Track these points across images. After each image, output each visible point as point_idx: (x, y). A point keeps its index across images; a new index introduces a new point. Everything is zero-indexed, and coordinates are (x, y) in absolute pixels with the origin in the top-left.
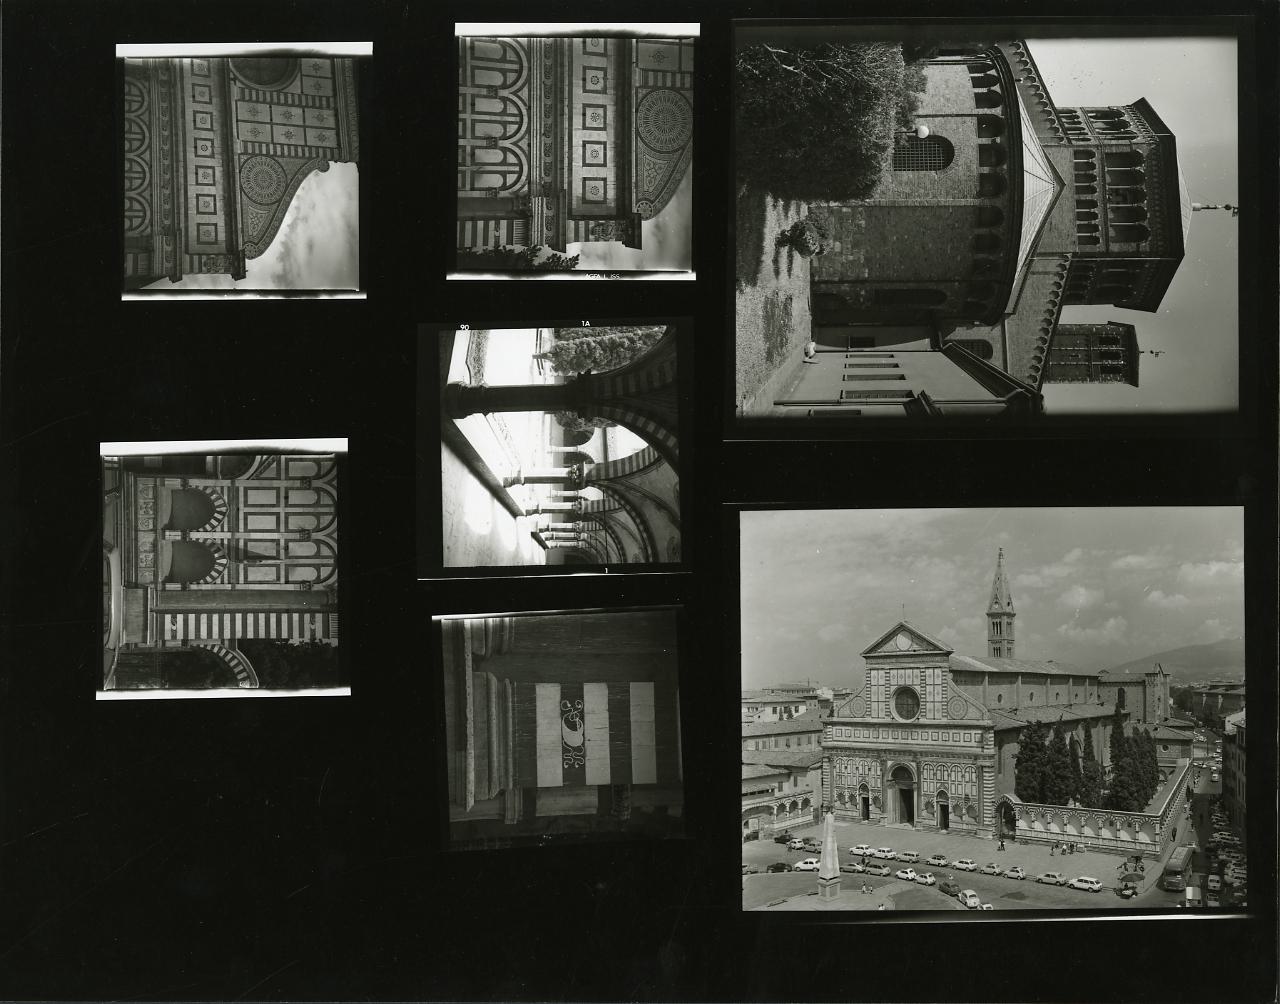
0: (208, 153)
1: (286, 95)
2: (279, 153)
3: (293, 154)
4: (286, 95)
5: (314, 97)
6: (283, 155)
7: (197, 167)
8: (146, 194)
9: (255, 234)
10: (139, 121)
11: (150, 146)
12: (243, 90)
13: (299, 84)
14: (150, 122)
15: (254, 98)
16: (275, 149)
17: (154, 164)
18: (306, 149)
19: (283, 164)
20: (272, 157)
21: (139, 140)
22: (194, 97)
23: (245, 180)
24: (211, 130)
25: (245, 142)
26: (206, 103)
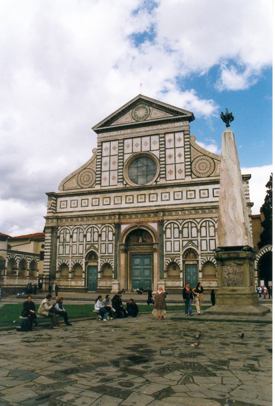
0: (193, 192)
1: (160, 158)
2: (189, 160)
3: (189, 153)
4: (160, 158)
5: (160, 145)
6: (190, 158)
11: (194, 219)
12: (161, 178)
13: (154, 151)
14: (183, 219)
15: (164, 172)
16: (187, 162)
17: (202, 217)
18: (186, 147)
19: (195, 157)
20: (191, 163)
21: (191, 223)
22: (167, 200)
24: (182, 192)
25: (186, 176)
26: (169, 195)
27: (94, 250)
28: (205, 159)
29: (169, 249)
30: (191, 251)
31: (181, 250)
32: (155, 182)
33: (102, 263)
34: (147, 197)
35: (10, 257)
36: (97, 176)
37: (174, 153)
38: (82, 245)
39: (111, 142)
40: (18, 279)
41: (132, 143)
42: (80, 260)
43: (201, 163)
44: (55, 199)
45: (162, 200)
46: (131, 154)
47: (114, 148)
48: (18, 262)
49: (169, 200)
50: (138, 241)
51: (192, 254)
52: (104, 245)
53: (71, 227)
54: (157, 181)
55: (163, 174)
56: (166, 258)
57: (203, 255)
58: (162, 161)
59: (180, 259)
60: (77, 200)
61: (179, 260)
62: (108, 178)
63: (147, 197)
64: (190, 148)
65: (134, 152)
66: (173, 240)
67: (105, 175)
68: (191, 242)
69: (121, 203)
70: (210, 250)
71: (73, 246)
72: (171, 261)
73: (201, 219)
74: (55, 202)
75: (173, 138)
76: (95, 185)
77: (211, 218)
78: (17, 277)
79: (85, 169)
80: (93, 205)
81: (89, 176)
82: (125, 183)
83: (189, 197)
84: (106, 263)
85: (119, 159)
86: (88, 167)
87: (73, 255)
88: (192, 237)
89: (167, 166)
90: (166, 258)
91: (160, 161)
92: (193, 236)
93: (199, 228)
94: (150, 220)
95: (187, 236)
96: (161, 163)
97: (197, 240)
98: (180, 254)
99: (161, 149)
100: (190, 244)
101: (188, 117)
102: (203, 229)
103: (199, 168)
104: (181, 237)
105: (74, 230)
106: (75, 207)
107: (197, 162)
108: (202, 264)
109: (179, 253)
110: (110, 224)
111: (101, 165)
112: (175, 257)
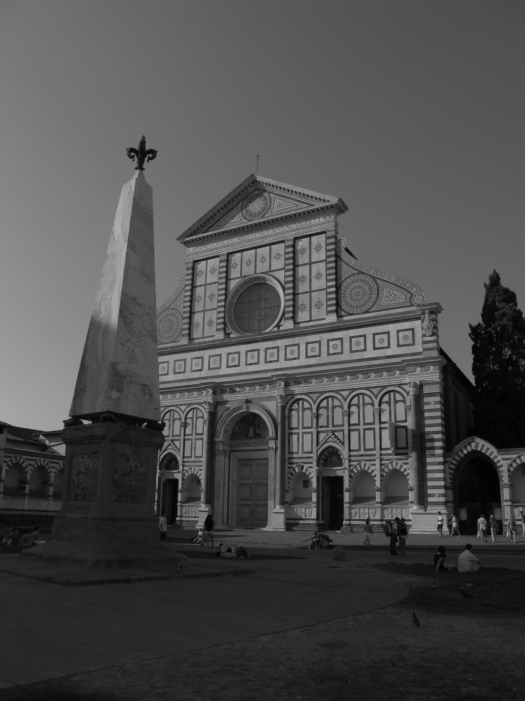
0: (338, 342)
1: (286, 283)
4: (286, 283)
5: (286, 259)
8: (376, 391)
9: (404, 297)
10: (318, 402)
11: (337, 391)
13: (276, 272)
18: (329, 260)
21: (333, 400)
22: (295, 359)
23: (358, 309)
24: (319, 342)
25: (328, 312)
28: (361, 280)
30: (333, 452)
32: (276, 327)
34: (262, 355)
35: (11, 460)
36: (185, 321)
37: (308, 273)
39: (208, 261)
40: (29, 499)
41: (242, 260)
43: (355, 288)
45: (286, 360)
46: (241, 279)
48: (29, 470)
49: (298, 358)
50: (248, 434)
51: (334, 458)
52: (190, 441)
55: (289, 312)
56: (290, 466)
57: (352, 458)
58: (289, 288)
61: (312, 470)
62: (202, 324)
63: (262, 355)
65: (243, 275)
66: (301, 431)
68: (333, 435)
70: (365, 450)
76: (180, 336)
77: (368, 389)
78: (27, 497)
79: (166, 309)
80: (176, 371)
83: (332, 351)
85: (220, 290)
86: (171, 307)
88: (334, 426)
89: (296, 296)
90: (290, 466)
91: (284, 289)
93: (346, 408)
95: (325, 424)
96: (287, 292)
97: (343, 431)
98: (312, 458)
99: (287, 268)
100: (330, 439)
101: (332, 206)
102: (354, 409)
103: (351, 297)
104: (315, 425)
107: (348, 286)
108: (350, 476)
110: (200, 404)
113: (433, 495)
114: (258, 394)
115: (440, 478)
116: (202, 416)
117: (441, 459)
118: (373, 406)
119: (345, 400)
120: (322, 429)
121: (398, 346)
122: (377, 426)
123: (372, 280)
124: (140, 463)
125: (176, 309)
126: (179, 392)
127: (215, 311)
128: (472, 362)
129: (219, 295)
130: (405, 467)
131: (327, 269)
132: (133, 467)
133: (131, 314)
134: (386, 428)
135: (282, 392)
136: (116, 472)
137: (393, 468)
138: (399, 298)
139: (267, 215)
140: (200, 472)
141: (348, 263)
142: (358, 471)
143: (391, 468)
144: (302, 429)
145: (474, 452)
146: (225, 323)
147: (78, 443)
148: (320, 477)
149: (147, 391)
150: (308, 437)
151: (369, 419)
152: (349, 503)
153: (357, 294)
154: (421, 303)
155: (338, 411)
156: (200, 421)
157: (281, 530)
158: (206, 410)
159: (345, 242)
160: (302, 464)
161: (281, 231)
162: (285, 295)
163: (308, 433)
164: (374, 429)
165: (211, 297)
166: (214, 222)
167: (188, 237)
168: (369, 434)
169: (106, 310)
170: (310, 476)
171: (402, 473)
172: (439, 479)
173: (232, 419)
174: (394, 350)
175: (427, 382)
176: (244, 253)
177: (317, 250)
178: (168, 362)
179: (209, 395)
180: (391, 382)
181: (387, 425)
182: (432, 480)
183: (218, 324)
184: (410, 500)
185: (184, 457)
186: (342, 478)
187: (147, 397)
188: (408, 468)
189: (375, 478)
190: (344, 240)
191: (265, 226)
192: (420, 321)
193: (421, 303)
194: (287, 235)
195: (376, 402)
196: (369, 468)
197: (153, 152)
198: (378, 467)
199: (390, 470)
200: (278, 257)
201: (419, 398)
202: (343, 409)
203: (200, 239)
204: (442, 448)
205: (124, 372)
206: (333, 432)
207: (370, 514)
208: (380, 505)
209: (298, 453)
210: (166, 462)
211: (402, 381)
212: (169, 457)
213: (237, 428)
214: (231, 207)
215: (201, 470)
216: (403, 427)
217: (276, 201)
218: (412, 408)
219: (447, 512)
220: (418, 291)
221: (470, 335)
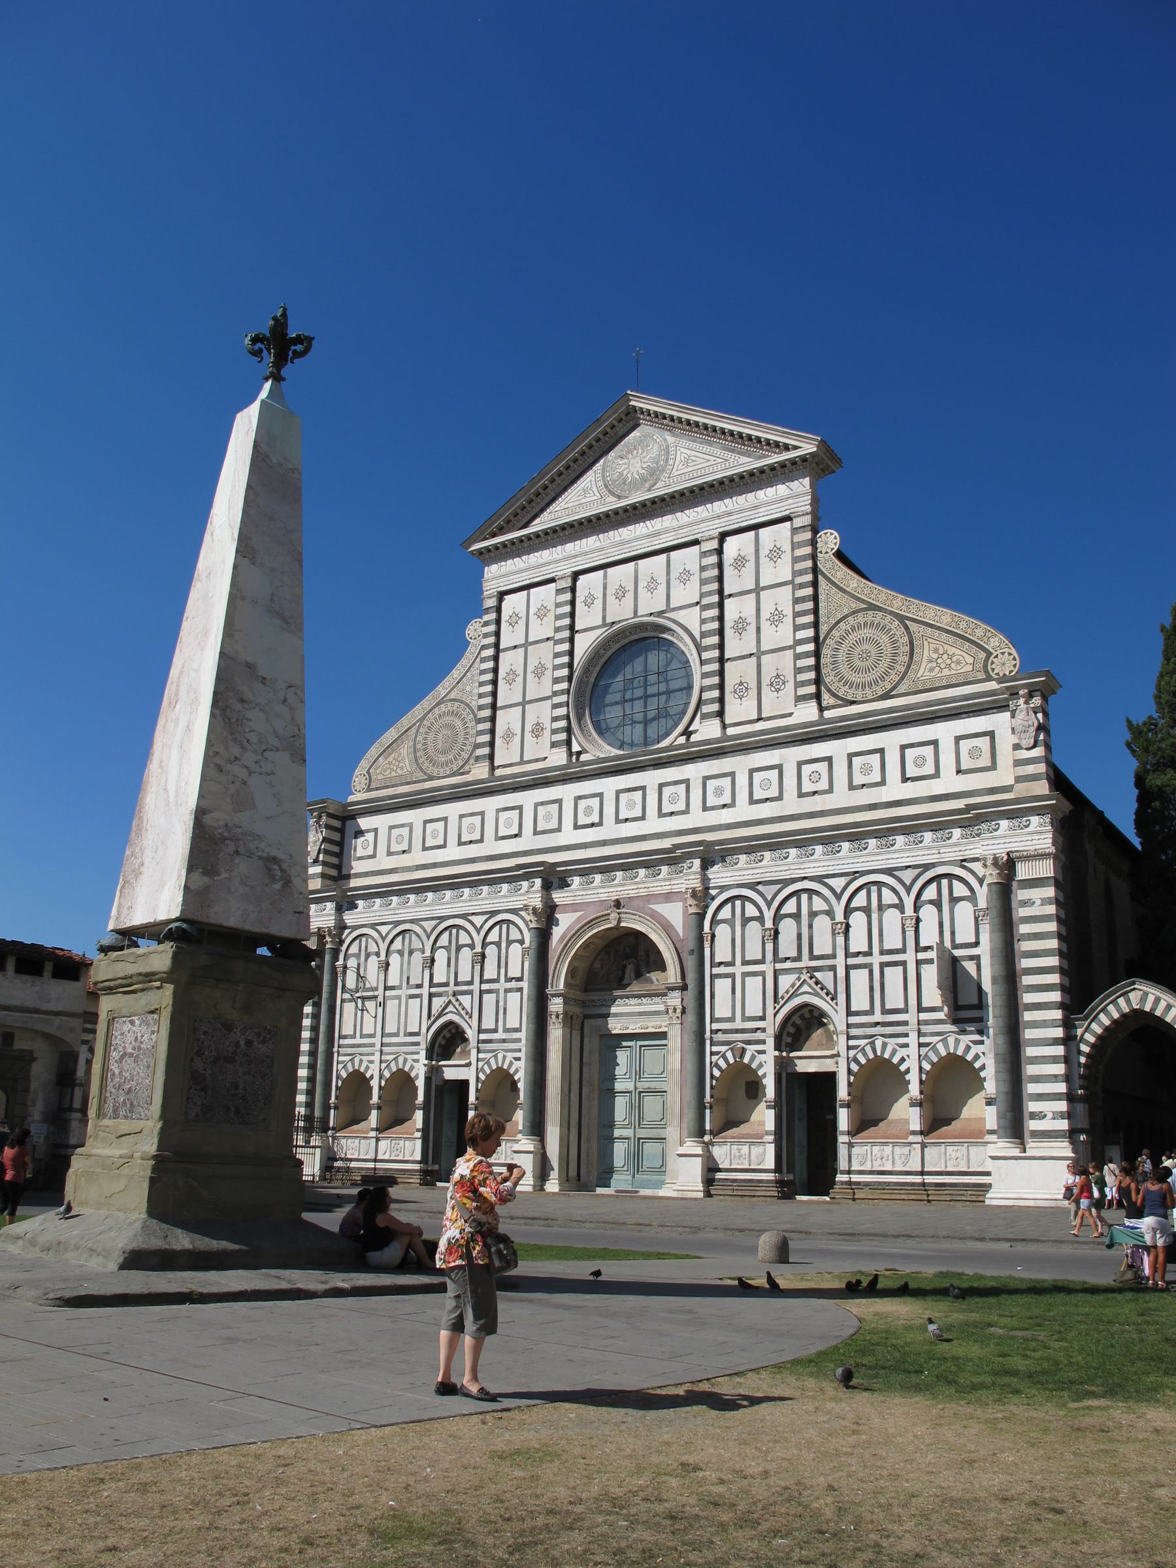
0: (822, 767)
1: (704, 635)
5: (703, 582)
7: (852, 787)
9: (970, 660)
11: (819, 879)
12: (705, 717)
13: (682, 612)
21: (810, 898)
22: (724, 806)
25: (799, 699)
27: (456, 1018)
28: (872, 625)
29: (723, 1010)
30: (813, 1017)
31: (770, 1011)
32: (682, 734)
33: (482, 1069)
34: (652, 798)
36: (481, 727)
37: (754, 612)
38: (418, 1000)
41: (605, 588)
42: (407, 1056)
43: (859, 642)
44: (336, 823)
47: (542, 613)
50: (622, 978)
52: (495, 995)
53: (384, 929)
54: (691, 729)
55: (712, 701)
56: (715, 1049)
57: (853, 1032)
59: (763, 1052)
60: (410, 825)
61: (762, 1057)
62: (519, 732)
63: (652, 798)
64: (815, 584)
65: (609, 620)
66: (738, 969)
67: (507, 720)
68: (811, 978)
69: (559, 830)
70: (885, 1012)
71: (389, 1003)
72: (731, 1061)
73: (848, 878)
74: (336, 836)
75: (753, 550)
76: (472, 761)
80: (463, 840)
81: (451, 727)
82: (576, 748)
83: (807, 787)
84: (498, 1068)
85: (557, 655)
86: (453, 695)
87: (386, 1040)
88: (812, 957)
89: (727, 665)
90: (715, 1049)
91: (700, 649)
92: (816, 953)
93: (840, 917)
94: (658, 891)
95: (794, 954)
96: (705, 655)
97: (833, 968)
98: (764, 1030)
100: (805, 988)
101: (804, 459)
102: (858, 921)
103: (849, 661)
104: (769, 956)
105: (392, 942)
106: (404, 852)
107: (843, 638)
108: (850, 1072)
109: (760, 1024)
110: (514, 911)
111: (495, 682)
112: (749, 1042)
113: (1041, 1116)
114: (643, 886)
115: (1056, 1076)
116: (520, 938)
117: (1059, 1032)
118: (903, 912)
119: (838, 897)
120: (788, 965)
121: (958, 772)
122: (910, 957)
123: (897, 622)
124: (258, 1034)
125: (462, 702)
126: (470, 885)
127: (549, 703)
128: (1136, 805)
129: (556, 668)
130: (976, 1049)
131: (797, 601)
132: (242, 1043)
133: (242, 701)
134: (930, 961)
135: (695, 881)
136: (200, 1053)
137: (949, 1054)
138: (958, 662)
139: (659, 484)
140: (516, 1064)
141: (842, 585)
142: (869, 1060)
143: (943, 1053)
144: (743, 965)
145: (1137, 1014)
146: (569, 730)
147: (121, 990)
148: (784, 1074)
149: (278, 873)
150: (754, 984)
151: (893, 940)
152: (848, 1133)
153: (865, 655)
154: (1011, 672)
155: (822, 923)
156: (516, 949)
157: (694, 1195)
158: (527, 925)
159: (835, 538)
160: (741, 1045)
161: (692, 518)
162: (702, 662)
163: (754, 974)
164: (903, 964)
165: (539, 672)
166: (542, 504)
167: (487, 539)
168: (894, 976)
169: (188, 693)
170: (760, 1073)
171: (970, 1064)
172: (1054, 1078)
173: (586, 945)
174: (949, 782)
175: (1025, 853)
176: (610, 571)
177: (771, 559)
178: (445, 819)
179: (535, 892)
180: (943, 855)
181: (932, 955)
182: (1037, 1079)
183: (554, 732)
184: (988, 1127)
185: (480, 1031)
186: (831, 1077)
187: (278, 886)
188: (983, 1053)
189: (907, 1077)
190: (832, 534)
191: (654, 510)
192: (1009, 713)
193: (1011, 672)
194: (703, 527)
195: (909, 902)
196: (894, 1052)
197: (306, 341)
198: (913, 1050)
199: (941, 1059)
200: (684, 577)
201: (1004, 891)
202: (833, 918)
203: (512, 542)
204: (1062, 1006)
205: (220, 831)
206: (812, 970)
207: (897, 1157)
208: (919, 1138)
209: (732, 1019)
210: (443, 1043)
211: (967, 852)
212: (450, 1031)
213: (598, 965)
214: (583, 468)
215: (518, 1059)
216: (971, 958)
217: (678, 452)
218: (994, 912)
219: (1073, 1155)
220: (1003, 645)
221: (1128, 745)
